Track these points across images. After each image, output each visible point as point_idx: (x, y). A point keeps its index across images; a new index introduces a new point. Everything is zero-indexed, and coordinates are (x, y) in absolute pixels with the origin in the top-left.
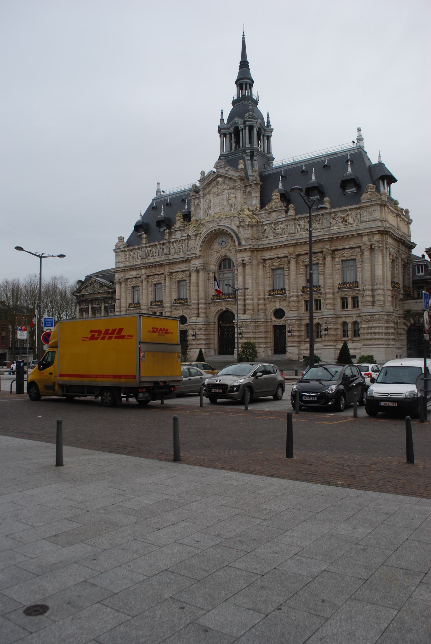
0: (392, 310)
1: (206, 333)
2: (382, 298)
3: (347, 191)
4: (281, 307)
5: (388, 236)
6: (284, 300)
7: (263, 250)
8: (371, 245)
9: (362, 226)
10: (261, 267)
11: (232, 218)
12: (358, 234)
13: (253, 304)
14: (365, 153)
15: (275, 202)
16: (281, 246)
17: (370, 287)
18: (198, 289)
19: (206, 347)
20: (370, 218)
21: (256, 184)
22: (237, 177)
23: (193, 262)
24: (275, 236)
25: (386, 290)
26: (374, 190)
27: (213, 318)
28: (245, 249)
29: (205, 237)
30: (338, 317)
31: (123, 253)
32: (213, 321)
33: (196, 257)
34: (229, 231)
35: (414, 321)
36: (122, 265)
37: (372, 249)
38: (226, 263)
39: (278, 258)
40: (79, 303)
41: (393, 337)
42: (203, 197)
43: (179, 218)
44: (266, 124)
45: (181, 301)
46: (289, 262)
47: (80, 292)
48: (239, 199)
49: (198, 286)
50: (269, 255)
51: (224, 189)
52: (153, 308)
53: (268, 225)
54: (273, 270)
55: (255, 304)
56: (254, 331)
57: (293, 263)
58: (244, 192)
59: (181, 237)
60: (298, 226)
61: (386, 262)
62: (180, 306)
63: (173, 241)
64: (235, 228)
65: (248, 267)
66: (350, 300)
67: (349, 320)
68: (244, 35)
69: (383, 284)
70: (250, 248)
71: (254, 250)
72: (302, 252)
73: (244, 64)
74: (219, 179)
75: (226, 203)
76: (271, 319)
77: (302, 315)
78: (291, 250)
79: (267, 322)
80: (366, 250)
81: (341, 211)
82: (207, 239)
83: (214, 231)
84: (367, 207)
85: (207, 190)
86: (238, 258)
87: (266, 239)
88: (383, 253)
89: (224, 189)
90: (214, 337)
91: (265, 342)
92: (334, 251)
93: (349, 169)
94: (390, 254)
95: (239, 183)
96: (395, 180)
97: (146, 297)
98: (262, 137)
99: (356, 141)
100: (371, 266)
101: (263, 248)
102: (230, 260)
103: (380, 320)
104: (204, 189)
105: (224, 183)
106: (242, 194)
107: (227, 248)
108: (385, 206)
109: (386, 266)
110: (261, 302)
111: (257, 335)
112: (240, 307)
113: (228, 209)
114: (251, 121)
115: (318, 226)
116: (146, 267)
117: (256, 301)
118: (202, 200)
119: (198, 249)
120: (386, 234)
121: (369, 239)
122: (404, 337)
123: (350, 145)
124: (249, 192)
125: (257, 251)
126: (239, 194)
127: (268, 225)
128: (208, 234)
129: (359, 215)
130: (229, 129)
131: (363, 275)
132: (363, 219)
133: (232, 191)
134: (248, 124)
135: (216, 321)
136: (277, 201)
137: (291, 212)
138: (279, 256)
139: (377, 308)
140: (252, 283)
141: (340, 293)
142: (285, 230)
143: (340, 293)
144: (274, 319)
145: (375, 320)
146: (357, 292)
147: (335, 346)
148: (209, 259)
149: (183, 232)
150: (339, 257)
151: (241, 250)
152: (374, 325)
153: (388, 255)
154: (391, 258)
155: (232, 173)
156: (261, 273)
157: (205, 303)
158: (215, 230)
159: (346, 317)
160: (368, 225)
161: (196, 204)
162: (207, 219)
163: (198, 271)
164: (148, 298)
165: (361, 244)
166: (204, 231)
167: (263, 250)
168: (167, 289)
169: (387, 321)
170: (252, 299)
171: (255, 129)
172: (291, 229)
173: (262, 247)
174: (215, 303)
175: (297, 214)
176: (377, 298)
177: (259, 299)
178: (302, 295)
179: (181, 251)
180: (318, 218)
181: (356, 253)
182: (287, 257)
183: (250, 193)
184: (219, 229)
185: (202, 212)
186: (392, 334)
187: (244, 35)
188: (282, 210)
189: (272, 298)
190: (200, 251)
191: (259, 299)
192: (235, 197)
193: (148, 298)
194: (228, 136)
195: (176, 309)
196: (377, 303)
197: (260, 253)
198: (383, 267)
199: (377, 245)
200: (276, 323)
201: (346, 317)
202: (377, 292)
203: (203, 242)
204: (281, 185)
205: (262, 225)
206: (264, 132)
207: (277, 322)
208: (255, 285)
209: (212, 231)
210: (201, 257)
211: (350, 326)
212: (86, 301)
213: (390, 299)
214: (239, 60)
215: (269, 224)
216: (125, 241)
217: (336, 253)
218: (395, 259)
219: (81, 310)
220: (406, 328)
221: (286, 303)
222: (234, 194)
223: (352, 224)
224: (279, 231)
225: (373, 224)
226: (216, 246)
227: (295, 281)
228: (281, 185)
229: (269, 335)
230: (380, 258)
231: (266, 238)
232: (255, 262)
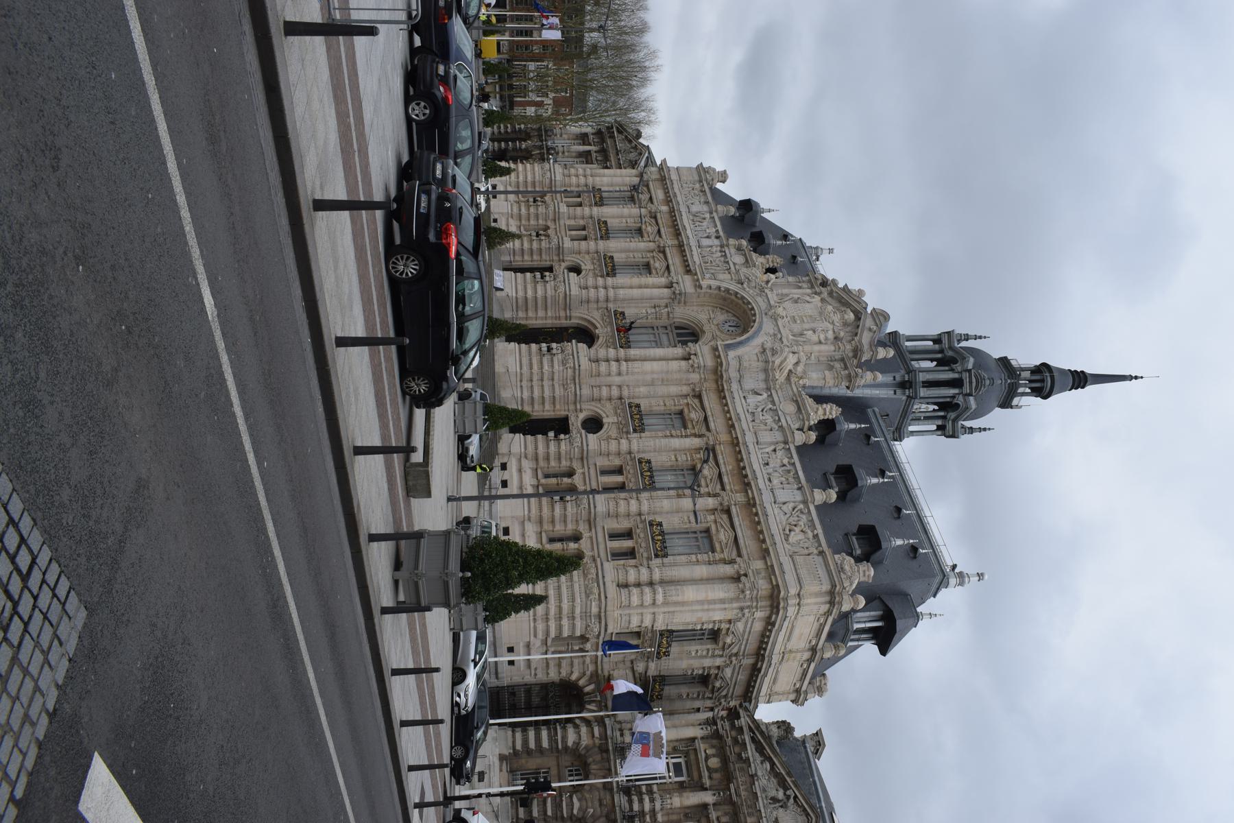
0: (609, 631)
1: (549, 301)
2: (635, 600)
3: (854, 538)
4: (605, 427)
5: (768, 613)
6: (620, 431)
7: (721, 392)
8: (746, 575)
9: (786, 560)
10: (685, 390)
12: (767, 551)
13: (609, 375)
14: (934, 589)
16: (730, 419)
17: (657, 576)
18: (637, 294)
19: (520, 301)
20: (803, 572)
21: (849, 376)
22: (860, 342)
23: (688, 278)
25: (652, 610)
26: (862, 579)
27: (578, 316)
28: (719, 356)
29: (737, 293)
30: (591, 523)
31: (697, 178)
32: (573, 314)
34: (752, 331)
35: (588, 693)
36: (674, 177)
37: (736, 579)
38: (688, 334)
39: (706, 419)
40: (599, 133)
41: (553, 634)
42: (816, 293)
44: (968, 424)
45: (610, 267)
46: (700, 436)
47: (619, 132)
48: (816, 348)
49: (640, 287)
50: (711, 401)
52: (594, 224)
54: (681, 413)
55: (609, 379)
56: (556, 377)
57: (697, 442)
58: (832, 359)
60: (773, 447)
61: (714, 610)
62: (600, 265)
64: (758, 341)
65: (683, 363)
66: (627, 544)
67: (584, 544)
68: (1136, 378)
69: (666, 603)
70: (721, 364)
71: (718, 373)
72: (720, 457)
73: (1080, 380)
74: (852, 316)
75: (806, 326)
76: (581, 411)
77: (591, 462)
78: (724, 437)
79: (575, 403)
80: (736, 566)
81: (812, 520)
84: (827, 565)
85: (829, 299)
86: (702, 350)
88: (731, 600)
89: (833, 323)
90: (542, 318)
91: (532, 398)
92: (728, 512)
93: (899, 542)
94: (730, 622)
95: (848, 347)
96: (884, 651)
97: (617, 214)
98: (942, 414)
99: (957, 570)
100: (701, 580)
101: (723, 390)
102: (696, 341)
103: (587, 596)
105: (845, 324)
108: (832, 603)
109: (703, 610)
110: (615, 392)
111: (546, 383)
112: (602, 353)
114: (971, 382)
115: (775, 481)
116: (672, 212)
117: (617, 380)
118: (809, 291)
119: (714, 283)
120: (772, 606)
121: (758, 572)
122: (553, 676)
123: (948, 561)
125: (717, 382)
126: (828, 349)
128: (743, 298)
129: (806, 552)
130: (951, 348)
131: (681, 566)
132: (798, 559)
133: (830, 335)
134: (965, 376)
135: (574, 321)
136: (820, 412)
137: (800, 438)
138: (710, 419)
139: (612, 589)
140: (652, 372)
141: (640, 526)
142: (763, 427)
143: (640, 526)
144: (582, 416)
145: (586, 586)
146: (645, 555)
147: (529, 519)
150: (715, 522)
151: (716, 349)
152: (576, 586)
153: (730, 615)
154: (724, 626)
155: (866, 338)
156: (674, 390)
157: (607, 300)
158: (753, 309)
159: (591, 538)
160: (788, 566)
162: (773, 298)
163: (670, 286)
164: (613, 217)
165: (746, 557)
166: (748, 293)
167: (721, 392)
168: (633, 245)
169: (586, 614)
170: (619, 374)
171: (956, 391)
172: (766, 437)
174: (610, 316)
175: (798, 448)
176: (635, 591)
177: (620, 387)
178: (633, 459)
180: (791, 480)
181: (726, 551)
182: (708, 429)
183: (831, 368)
184: (755, 315)
185: (785, 291)
186: (560, 628)
187: (1136, 378)
189: (624, 410)
191: (620, 387)
192: (820, 342)
193: (613, 217)
194: (937, 347)
195: (593, 259)
196: (624, 591)
197: (714, 386)
198: (701, 602)
199: (748, 585)
200: (572, 420)
201: (591, 538)
202: (647, 590)
203: (727, 290)
204: (852, 426)
205: (768, 389)
206: (950, 419)
207: (576, 422)
208: (648, 378)
209: (749, 303)
211: (572, 545)
212: (603, 141)
213: (635, 624)
214: (1088, 371)
215: (773, 403)
216: (719, 186)
217: (725, 517)
218: (721, 644)
219: (586, 135)
220: (574, 677)
221: (614, 433)
222: (826, 339)
223: (787, 540)
225: (790, 578)
226: (721, 317)
227: (664, 447)
228: (852, 426)
229: (547, 407)
230: (721, 595)
232: (695, 377)
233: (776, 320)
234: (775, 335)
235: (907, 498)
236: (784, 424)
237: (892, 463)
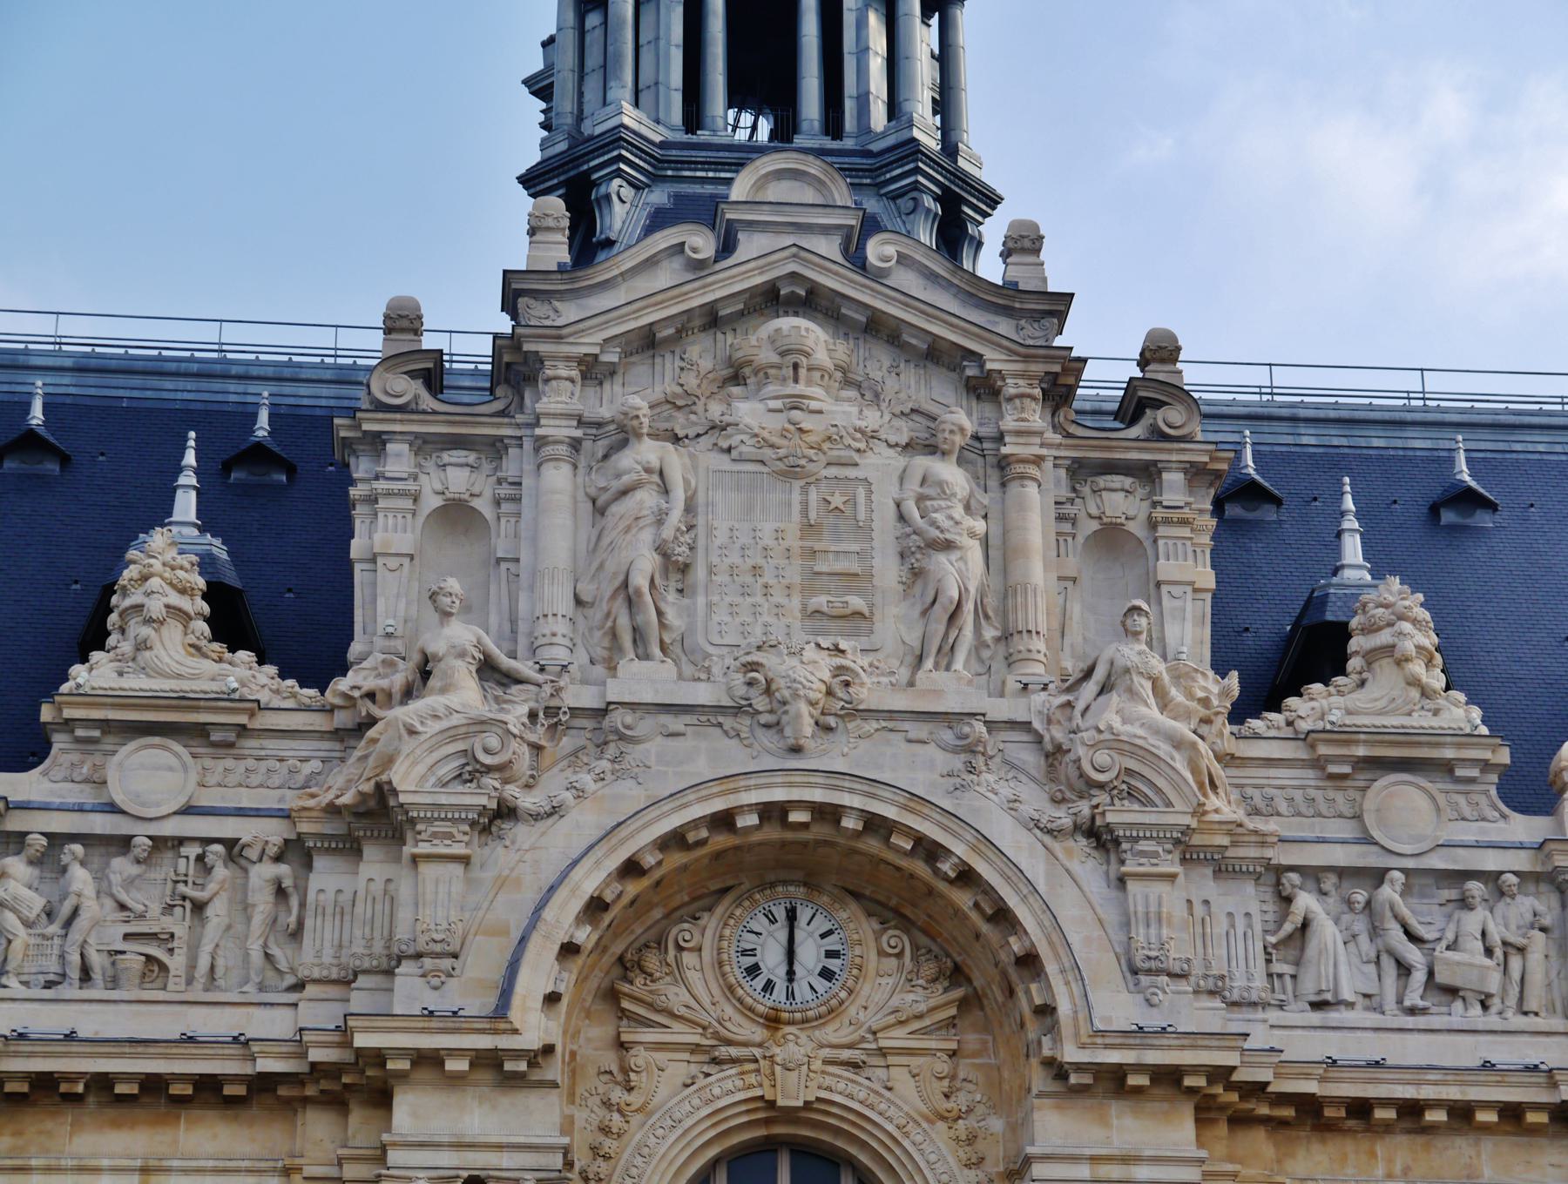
11: (980, 728)
15: (1414, 682)
16: (1512, 1114)
21: (1196, 473)
23: (413, 1111)
24: (1414, 998)
28: (1169, 1077)
33: (489, 1062)
43: (175, 599)
51: (873, 436)
53: (1329, 882)
59: (188, 810)
63: (57, 840)
75: (888, 571)
82: (633, 888)
83: (752, 820)
87: (1316, 1018)
104: (592, 371)
106: (1053, 526)
107: (833, 1032)
113: (913, 639)
124: (1111, 537)
125: (1240, 1121)
127: (1329, 882)
128: (675, 840)
148: (580, 1116)
149: (219, 766)
158: (773, 813)
161: (432, 502)
173: (1311, 1087)
179: (176, 963)
184: (828, 813)
188: (1486, 766)
190: (552, 999)
197: (1258, 1142)
210: (554, 1070)
215: (1342, 872)
224: (1467, 964)
231: (1318, 1006)
233: (855, 712)
234: (970, 748)
235: (1539, 443)
236: (1522, 861)
237: (1419, 442)
